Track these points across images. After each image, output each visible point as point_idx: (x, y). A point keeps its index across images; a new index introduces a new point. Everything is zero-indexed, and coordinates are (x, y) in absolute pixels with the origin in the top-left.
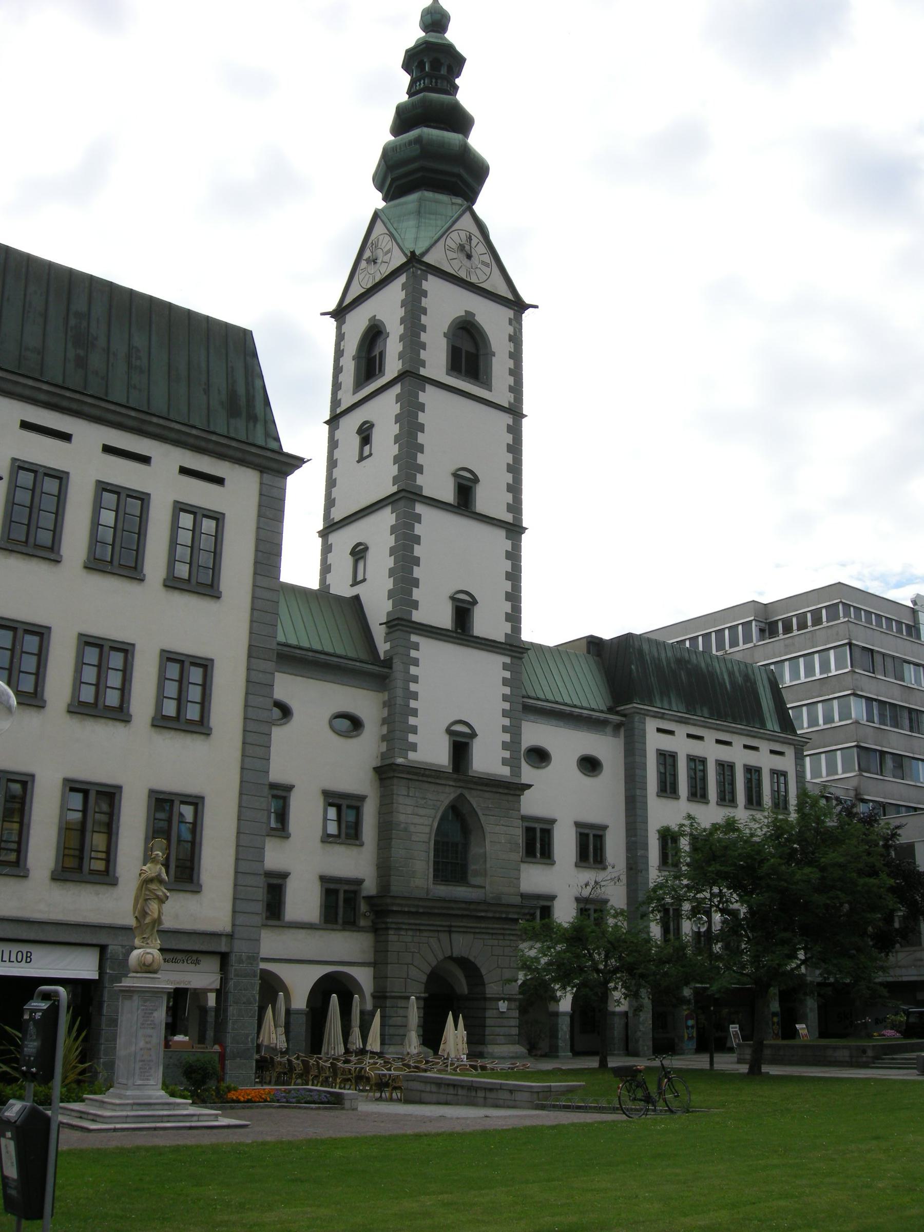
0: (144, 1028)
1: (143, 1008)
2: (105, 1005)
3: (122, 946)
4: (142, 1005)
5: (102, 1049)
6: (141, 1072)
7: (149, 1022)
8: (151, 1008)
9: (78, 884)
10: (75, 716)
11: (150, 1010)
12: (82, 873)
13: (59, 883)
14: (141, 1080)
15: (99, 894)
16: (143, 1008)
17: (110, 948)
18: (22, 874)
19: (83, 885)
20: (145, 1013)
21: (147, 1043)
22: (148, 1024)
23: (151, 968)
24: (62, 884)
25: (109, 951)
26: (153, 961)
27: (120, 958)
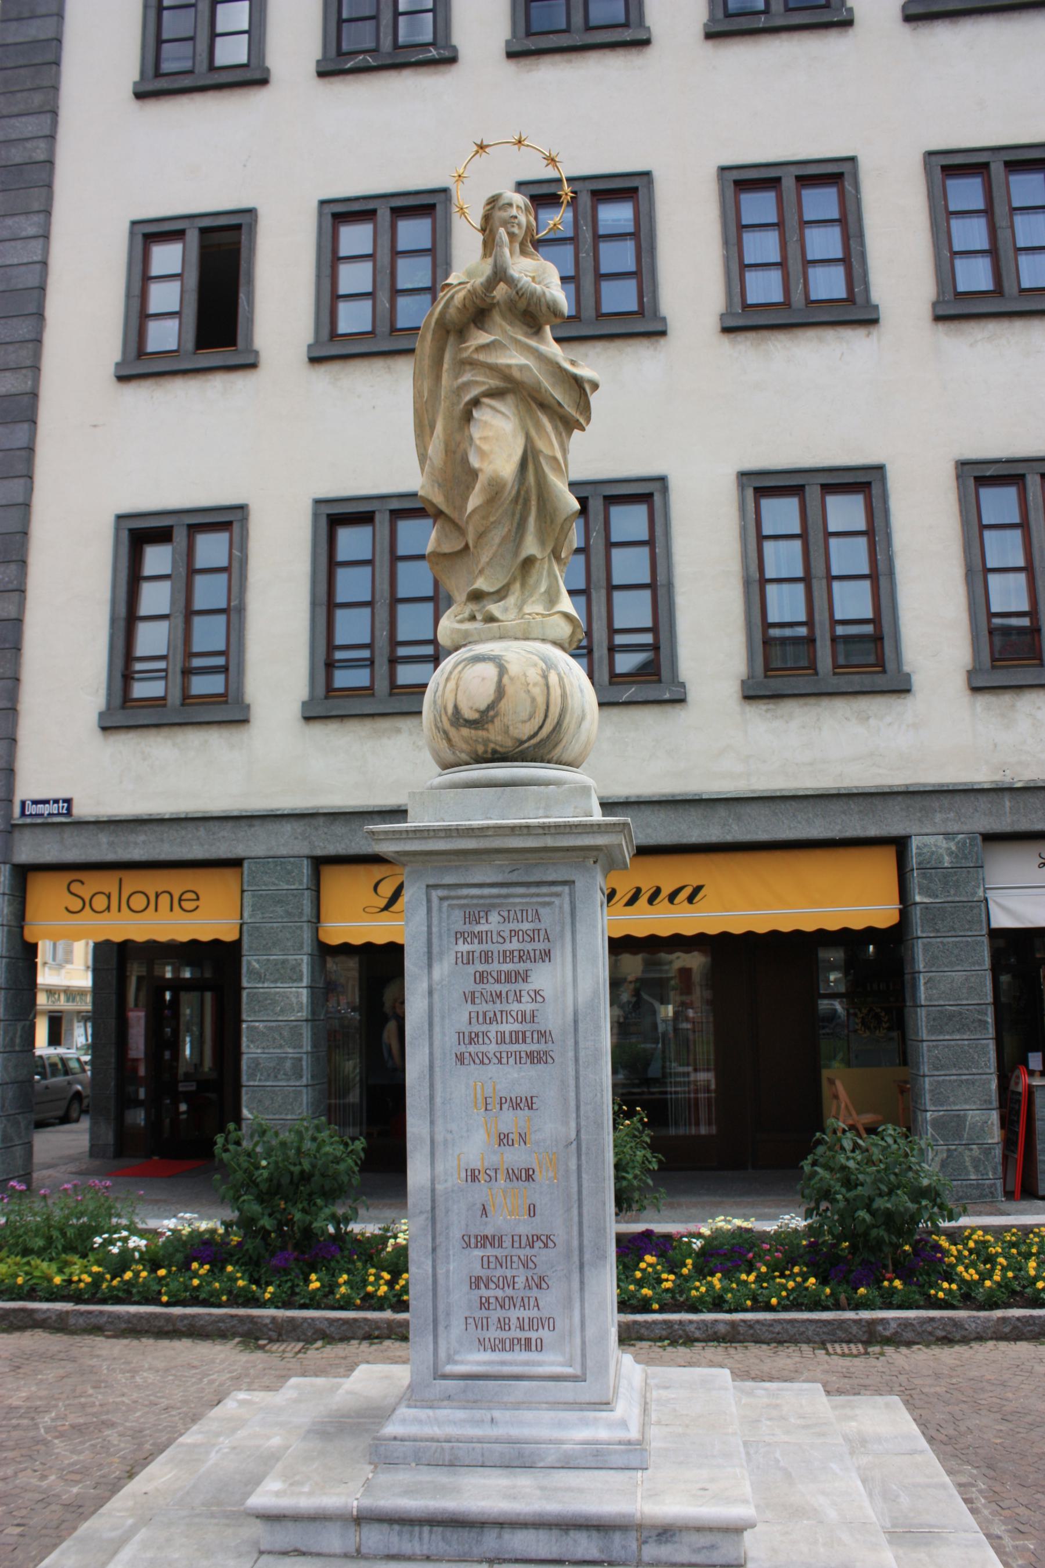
0: (482, 1060)
1: (463, 948)
2: (922, 981)
3: (948, 835)
4: (460, 935)
5: (927, 1086)
6: (484, 1304)
7: (507, 1028)
8: (515, 945)
9: (812, 701)
10: (741, 337)
11: (507, 956)
12: (816, 674)
13: (762, 707)
14: (483, 1344)
15: (868, 718)
16: (463, 948)
17: (915, 843)
18: (667, 696)
19: (825, 702)
20: (481, 978)
21: (504, 1139)
22: (501, 1039)
23: (495, 735)
24: (771, 706)
25: (914, 851)
26: (500, 691)
27: (946, 865)
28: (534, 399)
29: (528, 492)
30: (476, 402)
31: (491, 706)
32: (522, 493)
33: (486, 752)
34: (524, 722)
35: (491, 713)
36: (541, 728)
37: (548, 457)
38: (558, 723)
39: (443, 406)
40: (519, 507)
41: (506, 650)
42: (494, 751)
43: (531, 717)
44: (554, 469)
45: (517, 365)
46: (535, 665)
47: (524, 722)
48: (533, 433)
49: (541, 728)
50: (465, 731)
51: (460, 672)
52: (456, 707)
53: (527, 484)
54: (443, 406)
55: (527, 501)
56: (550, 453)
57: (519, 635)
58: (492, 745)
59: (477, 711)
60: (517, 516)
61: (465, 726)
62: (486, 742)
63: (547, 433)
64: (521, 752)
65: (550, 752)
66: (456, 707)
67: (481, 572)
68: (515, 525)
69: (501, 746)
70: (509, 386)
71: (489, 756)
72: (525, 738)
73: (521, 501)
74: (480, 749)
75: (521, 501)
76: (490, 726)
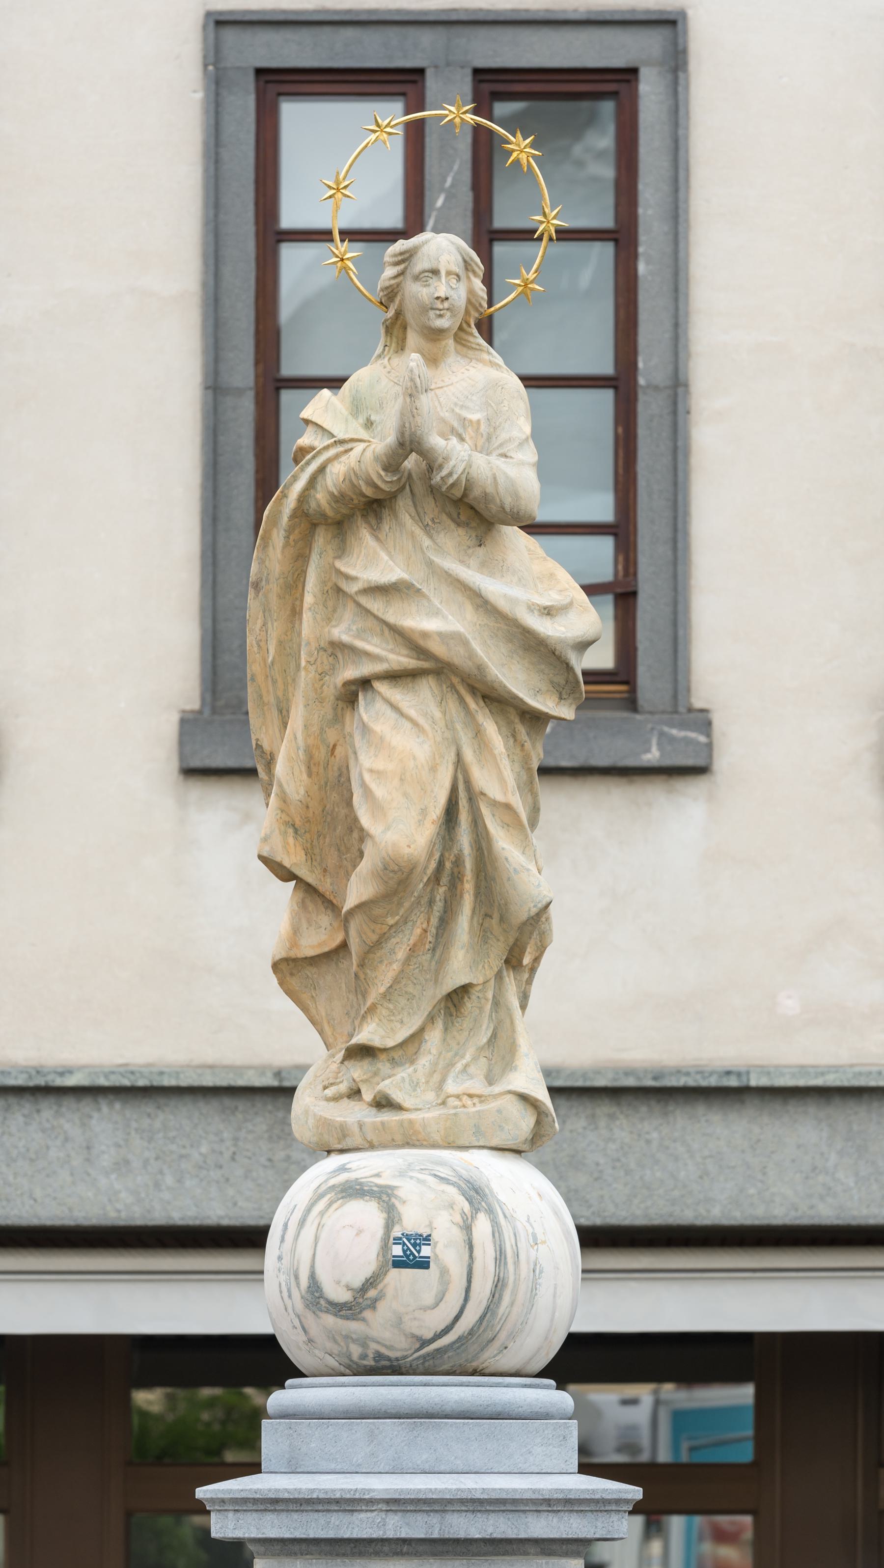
28: (473, 690)
29: (458, 862)
30: (365, 683)
31: (371, 1282)
32: (448, 865)
33: (364, 1356)
34: (425, 1309)
35: (372, 1293)
36: (457, 1318)
37: (494, 804)
38: (488, 1308)
39: (305, 678)
40: (442, 890)
41: (402, 1174)
42: (379, 1356)
43: (440, 1299)
44: (505, 825)
45: (440, 634)
46: (451, 1206)
47: (425, 1309)
48: (469, 755)
49: (457, 1318)
50: (330, 1320)
51: (322, 1214)
52: (313, 1276)
53: (455, 851)
54: (305, 678)
55: (456, 879)
56: (499, 797)
57: (437, 1137)
58: (374, 1346)
59: (349, 1288)
60: (439, 906)
61: (327, 1311)
62: (363, 1342)
63: (494, 757)
64: (425, 1357)
65: (476, 1357)
66: (313, 1276)
67: (372, 1009)
68: (434, 921)
69: (390, 1348)
70: (425, 665)
71: (370, 1362)
72: (429, 1335)
73: (445, 880)
74: (356, 1351)
75: (445, 880)
76: (367, 1314)
